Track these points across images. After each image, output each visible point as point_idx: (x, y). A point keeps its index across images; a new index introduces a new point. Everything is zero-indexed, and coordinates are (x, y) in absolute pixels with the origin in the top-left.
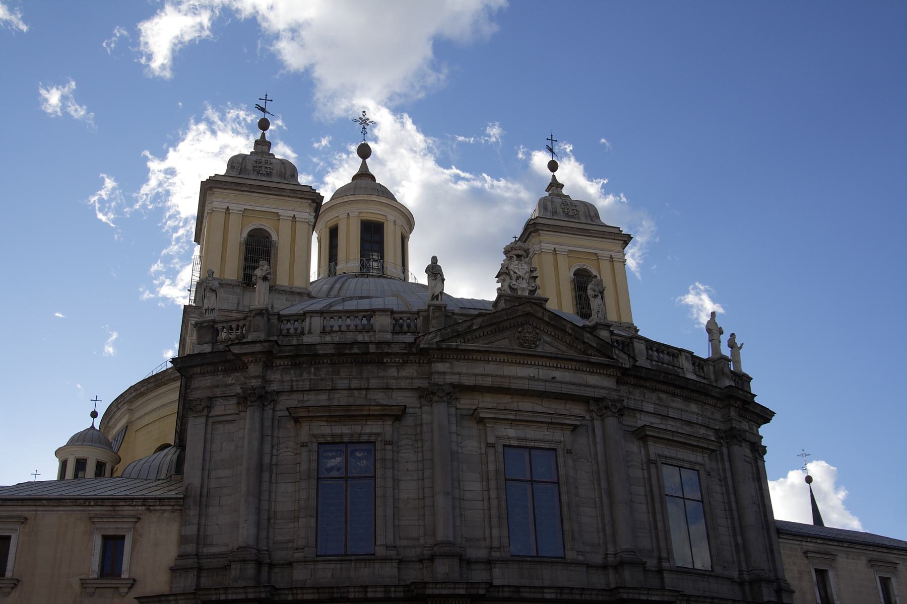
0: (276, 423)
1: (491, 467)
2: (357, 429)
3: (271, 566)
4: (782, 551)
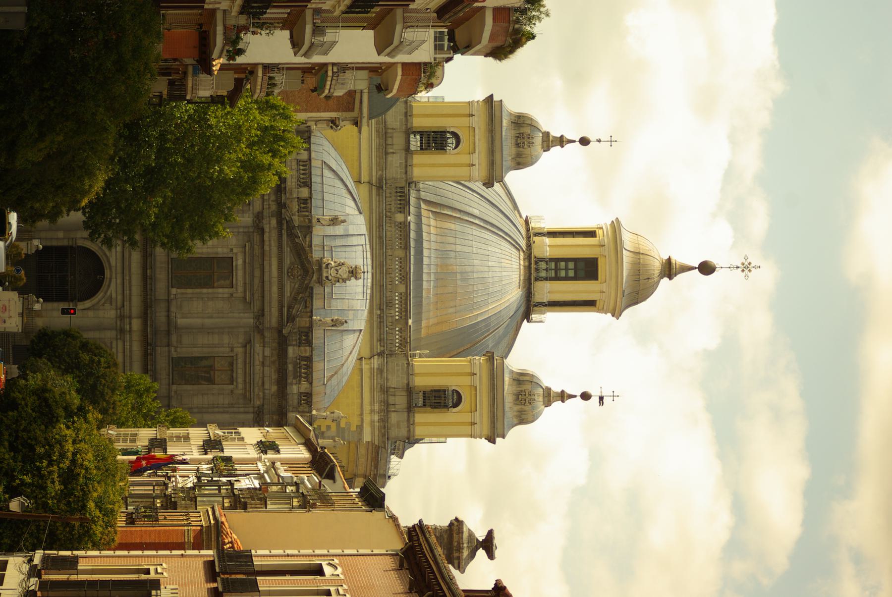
1: (220, 250)
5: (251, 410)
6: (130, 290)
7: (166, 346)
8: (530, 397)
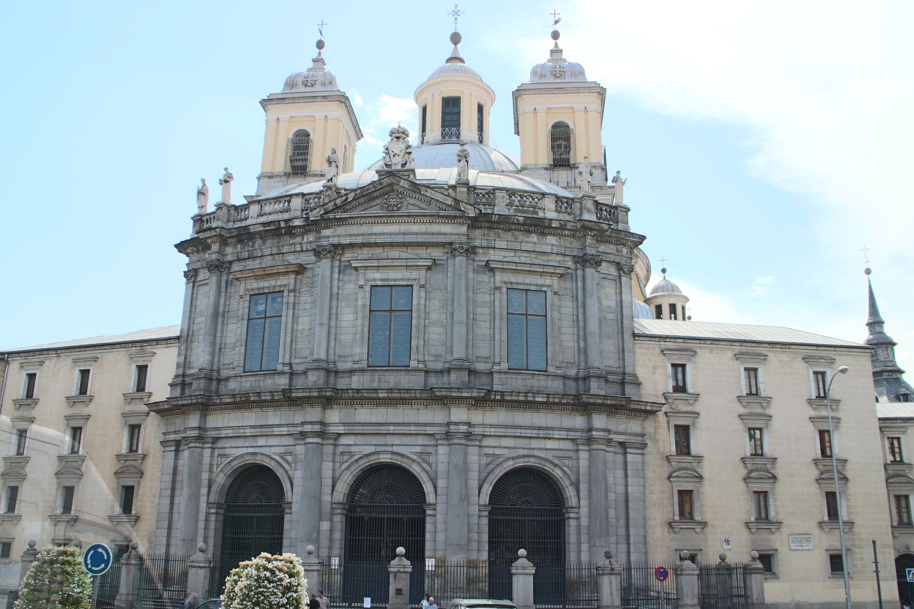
0: (229, 283)
1: (360, 303)
2: (273, 283)
3: (219, 380)
4: (637, 350)
5: (580, 273)
6: (409, 424)
7: (492, 378)
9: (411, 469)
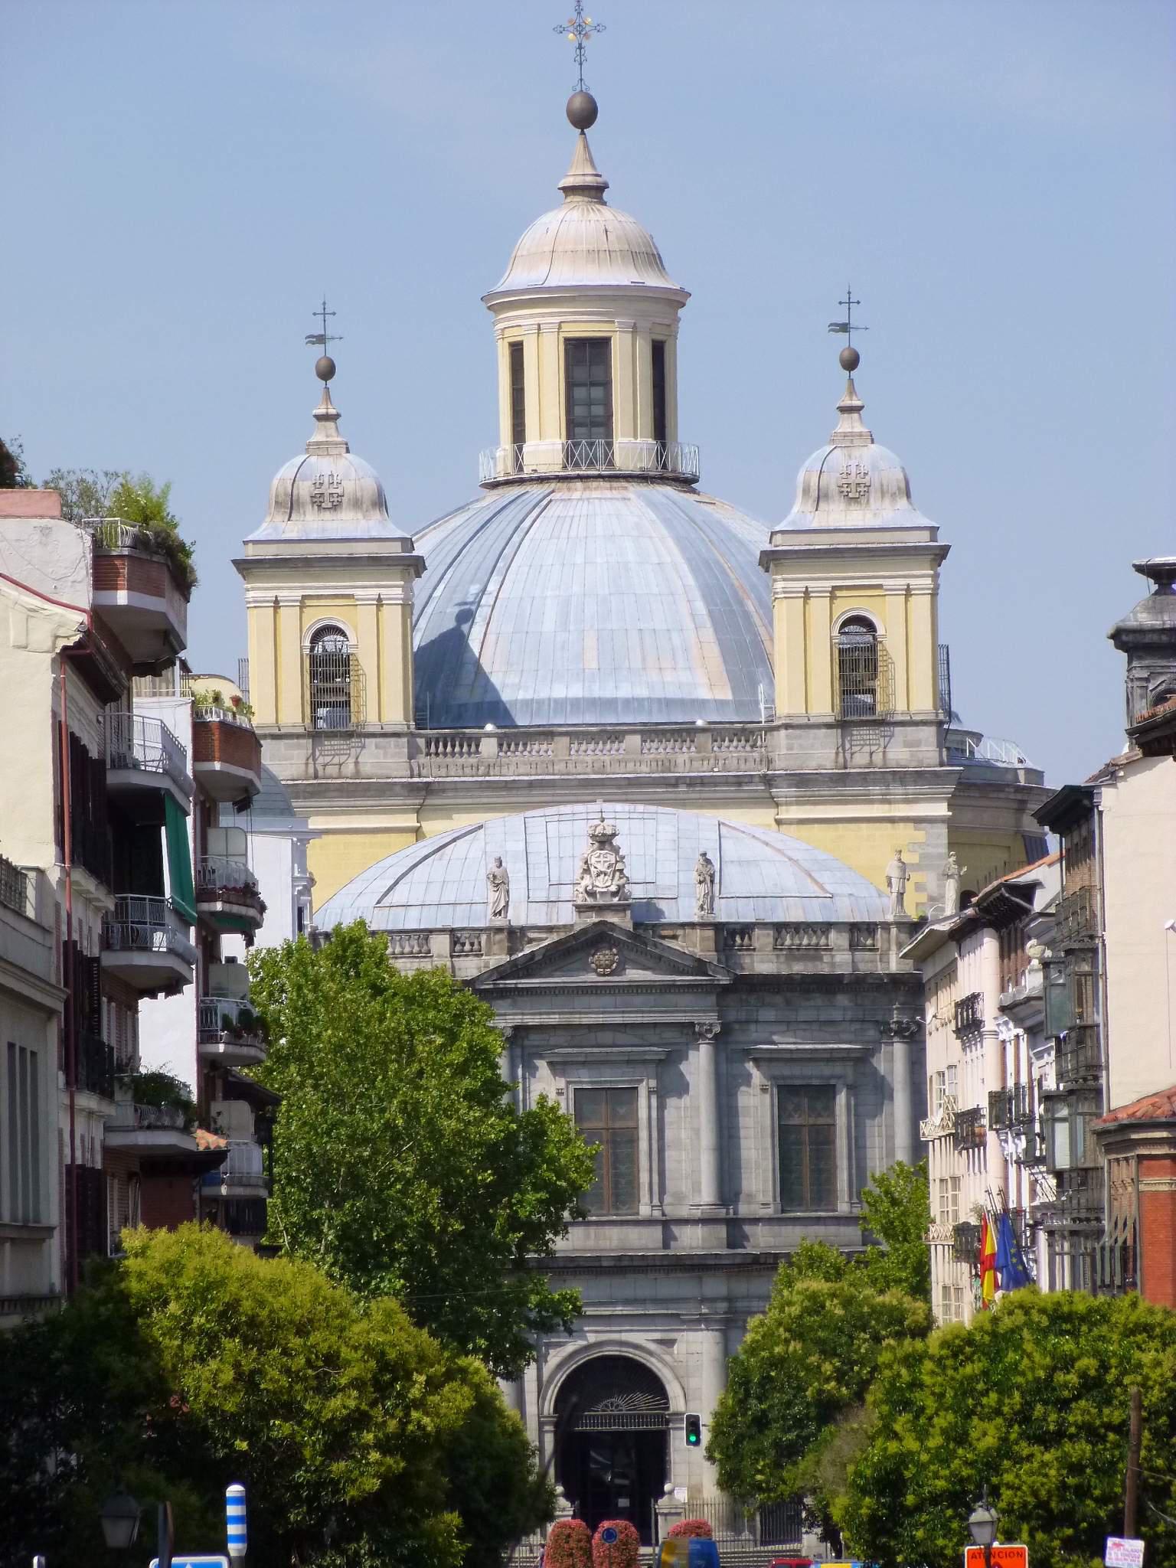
8: (853, 474)
9: (648, 1364)
